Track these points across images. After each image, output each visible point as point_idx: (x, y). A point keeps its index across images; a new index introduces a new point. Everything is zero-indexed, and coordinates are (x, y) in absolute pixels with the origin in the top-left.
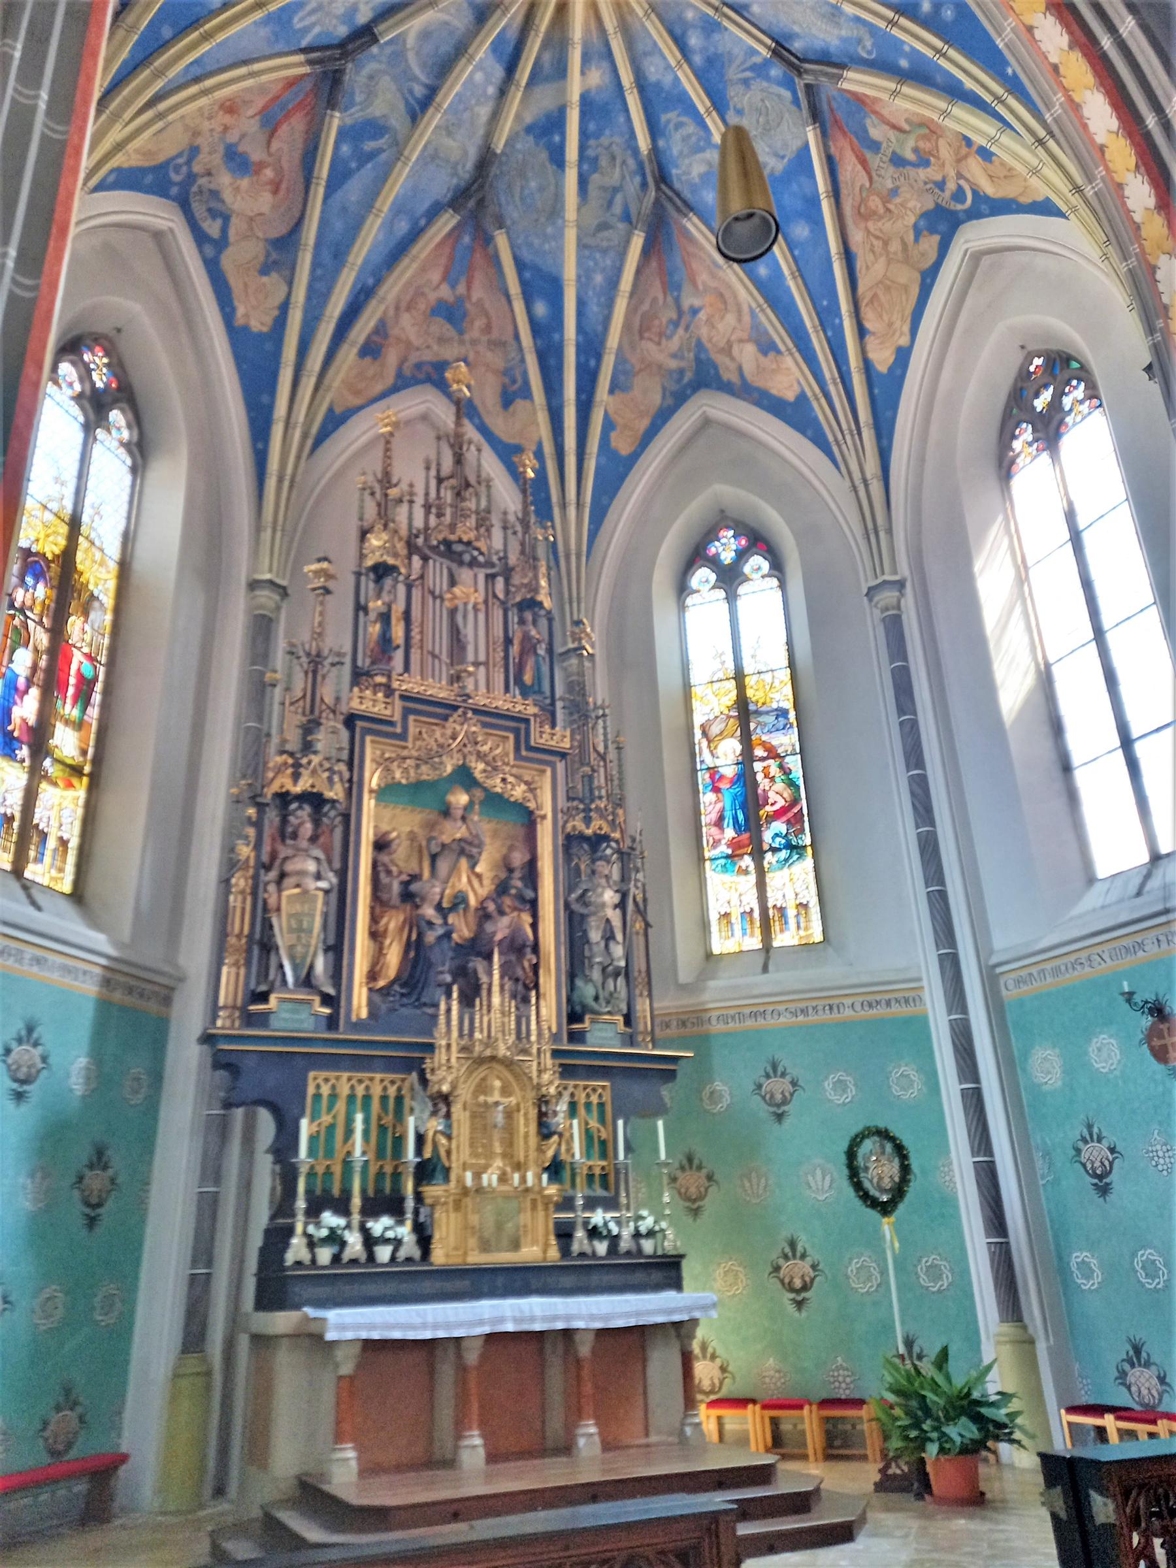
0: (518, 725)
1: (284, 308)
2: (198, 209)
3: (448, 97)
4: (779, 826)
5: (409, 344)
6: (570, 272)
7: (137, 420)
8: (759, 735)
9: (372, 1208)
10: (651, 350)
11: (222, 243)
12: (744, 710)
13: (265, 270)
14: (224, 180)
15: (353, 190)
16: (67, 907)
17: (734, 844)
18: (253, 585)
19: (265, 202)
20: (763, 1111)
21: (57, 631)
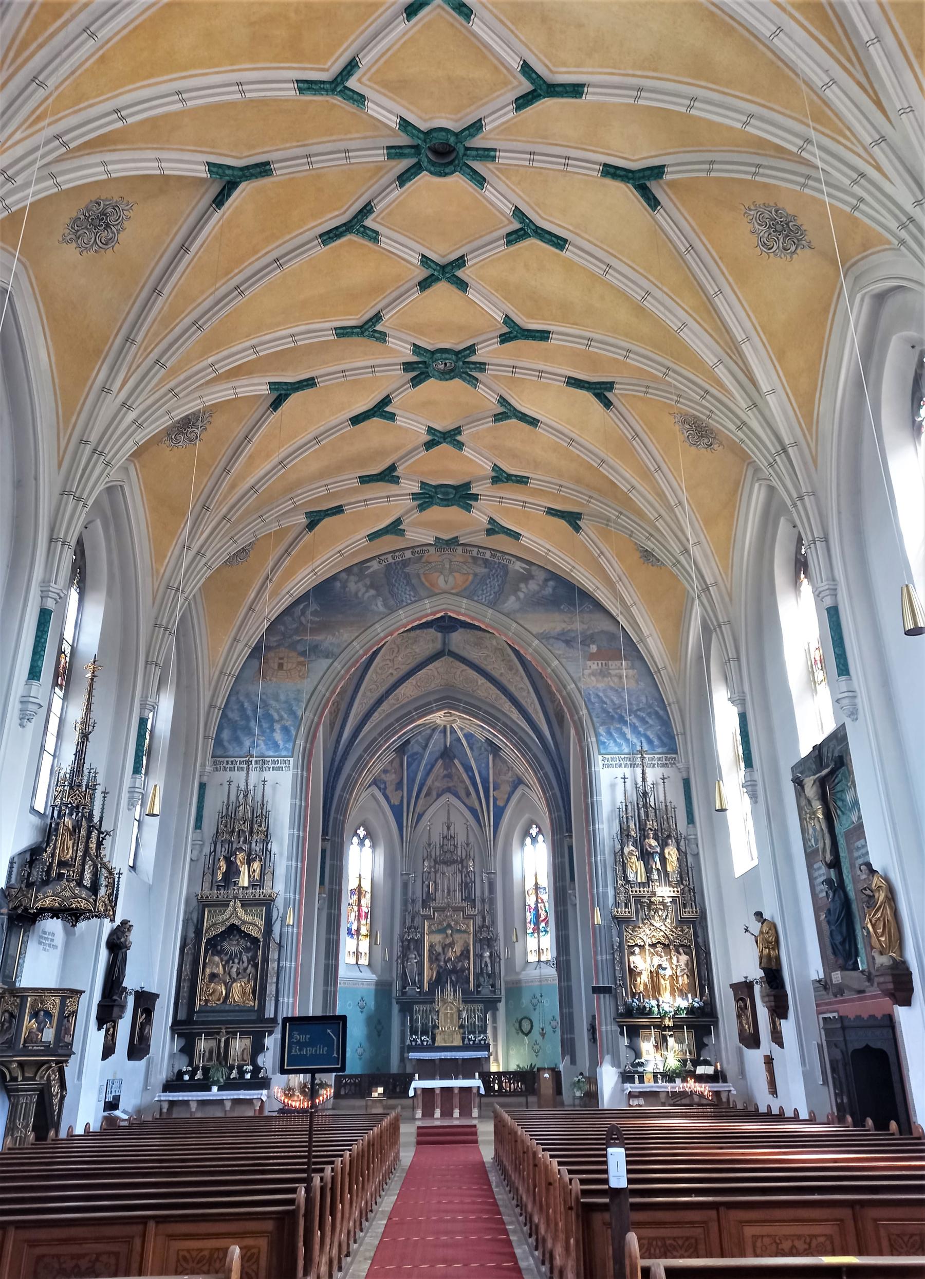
0: (462, 909)
1: (402, 797)
2: (378, 783)
3: (431, 746)
4: (543, 924)
5: (438, 788)
6: (474, 767)
7: (372, 840)
8: (540, 895)
9: (422, 1035)
10: (503, 777)
11: (385, 788)
12: (537, 887)
13: (396, 790)
14: (383, 776)
15: (414, 767)
16: (367, 969)
17: (534, 929)
18: (402, 874)
19: (393, 776)
20: (532, 1008)
21: (359, 906)
